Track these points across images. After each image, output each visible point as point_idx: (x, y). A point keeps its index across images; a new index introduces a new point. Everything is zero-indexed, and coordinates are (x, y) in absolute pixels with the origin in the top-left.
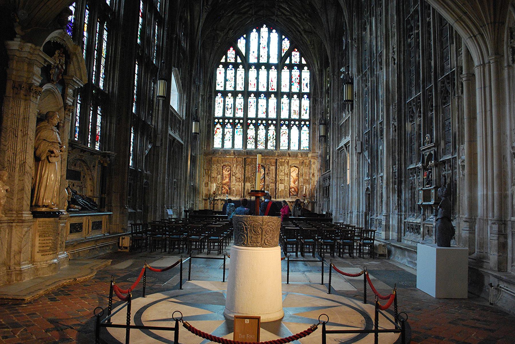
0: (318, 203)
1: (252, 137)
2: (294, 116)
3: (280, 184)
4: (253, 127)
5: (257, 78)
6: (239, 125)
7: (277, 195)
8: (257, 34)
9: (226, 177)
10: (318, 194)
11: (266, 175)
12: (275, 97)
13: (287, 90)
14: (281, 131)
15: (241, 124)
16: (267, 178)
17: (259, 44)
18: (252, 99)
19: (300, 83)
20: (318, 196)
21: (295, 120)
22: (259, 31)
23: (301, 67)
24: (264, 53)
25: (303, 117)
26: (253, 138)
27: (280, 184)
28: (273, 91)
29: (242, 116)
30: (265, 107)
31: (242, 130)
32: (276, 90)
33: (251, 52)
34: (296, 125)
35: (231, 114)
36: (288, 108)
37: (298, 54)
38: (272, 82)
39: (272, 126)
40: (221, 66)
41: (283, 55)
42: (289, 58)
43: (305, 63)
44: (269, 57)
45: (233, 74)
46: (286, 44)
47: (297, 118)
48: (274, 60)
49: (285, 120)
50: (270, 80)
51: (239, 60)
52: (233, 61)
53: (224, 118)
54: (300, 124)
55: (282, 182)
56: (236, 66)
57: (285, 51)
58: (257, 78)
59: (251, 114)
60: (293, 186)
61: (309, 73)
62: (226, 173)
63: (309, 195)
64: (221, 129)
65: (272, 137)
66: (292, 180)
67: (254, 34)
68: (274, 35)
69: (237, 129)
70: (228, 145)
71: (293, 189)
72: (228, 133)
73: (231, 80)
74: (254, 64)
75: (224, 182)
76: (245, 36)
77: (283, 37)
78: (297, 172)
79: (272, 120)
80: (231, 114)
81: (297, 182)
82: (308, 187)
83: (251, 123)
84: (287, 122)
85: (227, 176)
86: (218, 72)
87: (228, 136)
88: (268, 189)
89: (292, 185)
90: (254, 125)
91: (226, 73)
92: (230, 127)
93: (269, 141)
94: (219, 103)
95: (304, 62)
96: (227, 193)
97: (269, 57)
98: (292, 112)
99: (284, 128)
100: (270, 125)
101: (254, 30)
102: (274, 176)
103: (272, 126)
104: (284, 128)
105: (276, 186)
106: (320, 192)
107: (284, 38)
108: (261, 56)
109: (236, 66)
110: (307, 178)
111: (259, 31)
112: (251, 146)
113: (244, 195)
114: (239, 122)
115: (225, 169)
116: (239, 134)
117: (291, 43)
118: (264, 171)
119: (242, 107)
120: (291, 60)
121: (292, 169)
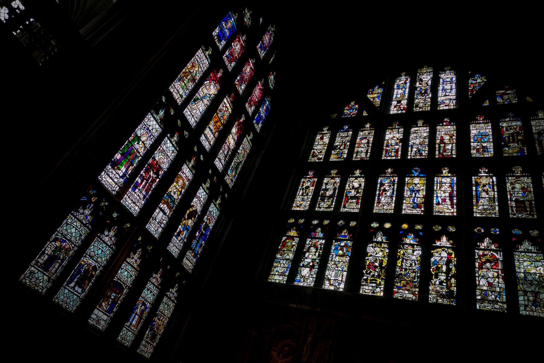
1: (377, 264)
6: (345, 232)
15: (351, 230)
31: (350, 243)
53: (311, 213)
72: (313, 249)
87: (311, 256)
90: (386, 232)
92: (321, 235)
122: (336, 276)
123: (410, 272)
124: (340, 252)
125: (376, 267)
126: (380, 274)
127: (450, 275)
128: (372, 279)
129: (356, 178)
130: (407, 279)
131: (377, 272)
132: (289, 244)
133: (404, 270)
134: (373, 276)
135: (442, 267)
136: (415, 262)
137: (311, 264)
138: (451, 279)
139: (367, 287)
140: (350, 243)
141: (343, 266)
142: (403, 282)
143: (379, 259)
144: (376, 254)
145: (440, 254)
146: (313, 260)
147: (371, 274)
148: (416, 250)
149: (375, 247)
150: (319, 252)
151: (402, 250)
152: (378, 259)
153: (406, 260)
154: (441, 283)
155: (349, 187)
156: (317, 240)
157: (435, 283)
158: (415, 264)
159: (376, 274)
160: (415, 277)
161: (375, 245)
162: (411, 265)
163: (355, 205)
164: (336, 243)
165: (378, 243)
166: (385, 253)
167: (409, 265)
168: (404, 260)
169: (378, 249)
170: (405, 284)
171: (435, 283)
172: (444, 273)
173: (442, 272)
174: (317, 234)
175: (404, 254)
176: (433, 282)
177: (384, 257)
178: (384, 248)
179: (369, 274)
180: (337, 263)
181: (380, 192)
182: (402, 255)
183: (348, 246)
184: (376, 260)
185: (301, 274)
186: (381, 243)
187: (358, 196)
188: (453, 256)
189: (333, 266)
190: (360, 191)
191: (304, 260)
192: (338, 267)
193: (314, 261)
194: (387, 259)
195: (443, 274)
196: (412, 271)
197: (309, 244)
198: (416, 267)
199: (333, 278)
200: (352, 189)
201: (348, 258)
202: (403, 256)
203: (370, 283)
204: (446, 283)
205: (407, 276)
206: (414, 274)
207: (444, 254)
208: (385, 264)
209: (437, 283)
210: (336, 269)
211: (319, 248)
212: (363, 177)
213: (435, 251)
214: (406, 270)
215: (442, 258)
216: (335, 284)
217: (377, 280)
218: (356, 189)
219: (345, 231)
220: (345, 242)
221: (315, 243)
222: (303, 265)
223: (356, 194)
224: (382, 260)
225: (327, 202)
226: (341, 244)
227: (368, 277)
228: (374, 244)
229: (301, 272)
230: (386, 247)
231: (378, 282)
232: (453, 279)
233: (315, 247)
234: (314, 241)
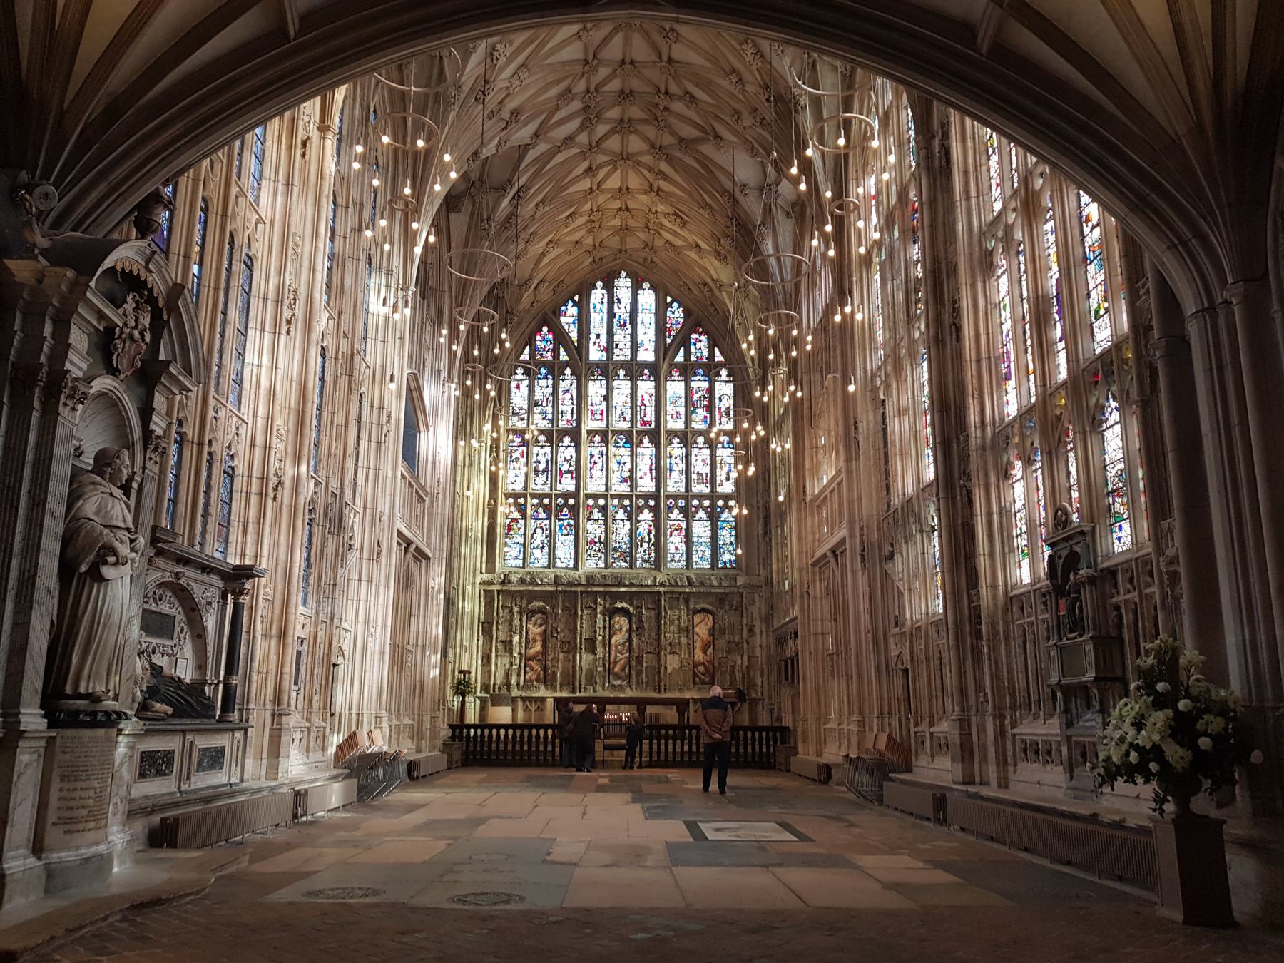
0: (766, 701)
1: (597, 540)
2: (699, 488)
3: (669, 657)
4: (600, 515)
5: (607, 398)
7: (662, 684)
8: (604, 291)
9: (535, 641)
10: (765, 679)
11: (634, 634)
12: (651, 442)
13: (680, 425)
14: (670, 523)
16: (635, 639)
17: (611, 315)
18: (593, 450)
19: (710, 408)
20: (765, 684)
21: (701, 497)
22: (609, 287)
23: (711, 370)
24: (622, 337)
25: (719, 490)
26: (601, 543)
27: (668, 656)
28: (648, 427)
29: (572, 488)
30: (628, 466)
31: (572, 522)
32: (653, 426)
33: (593, 337)
34: (705, 509)
35: (545, 484)
36: (682, 466)
37: (704, 338)
38: (643, 408)
39: (646, 511)
40: (520, 371)
41: (669, 341)
42: (682, 349)
43: (722, 359)
44: (635, 347)
45: (550, 390)
46: (676, 314)
47: (707, 490)
48: (647, 355)
49: (676, 497)
50: (639, 403)
51: (563, 357)
52: (548, 356)
54: (713, 506)
55: (674, 649)
56: (555, 371)
57: (673, 333)
58: (607, 398)
59: (594, 484)
61: (731, 385)
62: (535, 630)
63: (743, 681)
64: (522, 522)
65: (646, 539)
66: (698, 644)
67: (598, 296)
68: (647, 298)
69: (560, 520)
70: (539, 559)
71: (701, 668)
72: (539, 531)
73: (544, 404)
74: (598, 365)
75: (532, 652)
76: (576, 298)
77: (669, 299)
78: (710, 624)
79: (646, 497)
80: (545, 484)
81: (710, 650)
82: (739, 662)
83: (596, 505)
84: (682, 503)
85: (538, 638)
86: (513, 384)
88: (639, 668)
89: (699, 656)
91: (531, 389)
93: (640, 549)
94: (517, 459)
95: (719, 357)
96: (538, 680)
97: (635, 347)
98: (694, 476)
99: (675, 514)
100: (640, 509)
101: (599, 284)
102: (654, 635)
103: (646, 511)
104: (675, 514)
105: (659, 660)
106: (769, 674)
107: (672, 302)
108: (617, 345)
109: (555, 371)
110: (737, 638)
111: (609, 287)
112: (593, 564)
114: (566, 504)
115: (533, 619)
116: (565, 532)
117: (687, 313)
118: (630, 623)
119: (572, 468)
120: (688, 353)
121: (698, 618)
124: (565, 532)
140: (572, 522)
146: (542, 542)
186: (597, 520)
198: (626, 540)
207: (647, 527)
233: (541, 528)
234: (539, 522)
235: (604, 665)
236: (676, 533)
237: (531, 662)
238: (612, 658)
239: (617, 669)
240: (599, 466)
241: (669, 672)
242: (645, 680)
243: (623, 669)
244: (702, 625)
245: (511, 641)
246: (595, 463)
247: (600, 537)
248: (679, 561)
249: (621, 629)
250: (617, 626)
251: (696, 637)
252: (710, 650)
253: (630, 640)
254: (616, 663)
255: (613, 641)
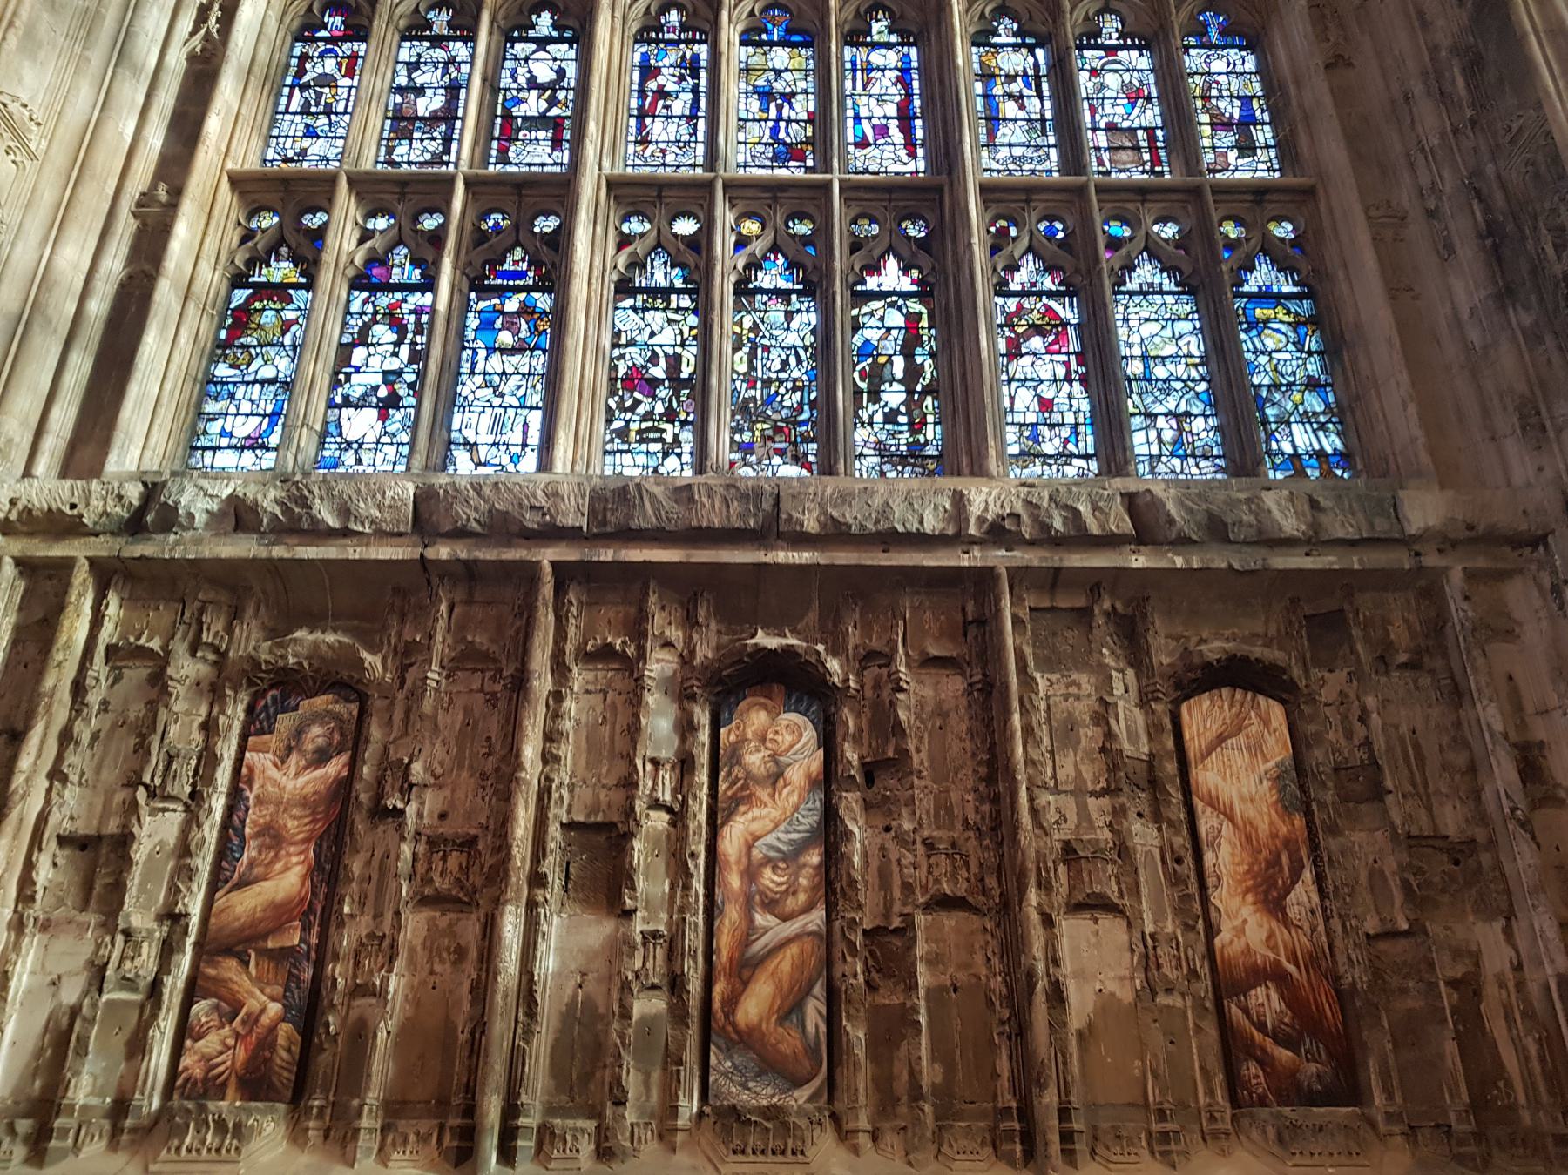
1: (658, 372)
9: (273, 837)
60: (1263, 954)
66: (1225, 858)
71: (1266, 1000)
75: (244, 904)
78: (1278, 748)
81: (1303, 896)
82: (1497, 959)
85: (294, 825)
105: (1012, 945)
110: (1452, 820)
113: (511, 1110)
115: (285, 722)
118: (828, 742)
122: (498, 426)
123: (782, 390)
124: (506, 338)
125: (654, 383)
126: (675, 404)
127: (919, 388)
128: (644, 425)
129: (542, 43)
130: (775, 416)
131: (663, 400)
132: (268, 318)
133: (759, 384)
134: (648, 416)
135: (890, 361)
136: (797, 354)
137: (383, 392)
138: (921, 401)
139: (627, 458)
141: (521, 392)
142: (759, 426)
143: (666, 355)
144: (652, 334)
145: (882, 319)
147: (641, 410)
148: (798, 311)
149: (645, 310)
150: (414, 343)
151: (748, 312)
152: (661, 354)
153: (767, 349)
154: (890, 417)
155: (515, 80)
156: (398, 296)
157: (871, 417)
158: (799, 361)
159: (660, 408)
160: (801, 404)
161: (644, 301)
162: (785, 364)
163: (548, 150)
164: (482, 305)
165: (653, 292)
166: (686, 330)
167: (777, 365)
168: (760, 350)
169: (656, 319)
170: (770, 433)
171: (871, 417)
172: (900, 381)
173: (892, 380)
174: (396, 271)
175: (755, 328)
176: (866, 418)
177: (683, 345)
178: (678, 309)
179: (632, 409)
180: (496, 379)
181: (644, 100)
182: (750, 330)
183: (534, 312)
184: (654, 359)
185: (340, 435)
186: (666, 293)
187: (558, 117)
188: (924, 323)
189: (479, 393)
190: (561, 95)
191: (348, 379)
192: (502, 395)
193: (392, 378)
194: (694, 350)
195: (896, 386)
196: (790, 385)
197: (363, 313)
199: (490, 439)
200: (529, 90)
201: (542, 359)
202: (752, 335)
203: (640, 441)
204: (909, 413)
205: (775, 405)
206: (798, 394)
207: (896, 319)
208: (691, 369)
209: (879, 418)
210: (497, 401)
211: (410, 327)
212: (570, 42)
213: (865, 310)
214: (767, 383)
215: (889, 330)
216: (496, 461)
217: (663, 431)
218: (542, 88)
219: (518, 253)
220: (522, 296)
221: (391, 307)
222: (346, 398)
223: (548, 110)
224: (678, 358)
225: (422, 140)
226: (503, 304)
227: (627, 422)
228: (639, 297)
229: (339, 426)
230: (686, 309)
231: (669, 438)
232: (929, 401)
234: (384, 300)
235: (676, 984)
236: (1036, 343)
237: (229, 969)
238: (725, 942)
239: (755, 1006)
240: (680, 106)
241: (1076, 1021)
242: (929, 1074)
243: (790, 1010)
244: (1235, 754)
245: (125, 840)
246: (662, 93)
247: (675, 362)
248: (1065, 457)
249: (776, 777)
250: (755, 759)
251: (1207, 822)
252: (1303, 896)
253: (830, 831)
254: (746, 968)
255: (732, 840)
